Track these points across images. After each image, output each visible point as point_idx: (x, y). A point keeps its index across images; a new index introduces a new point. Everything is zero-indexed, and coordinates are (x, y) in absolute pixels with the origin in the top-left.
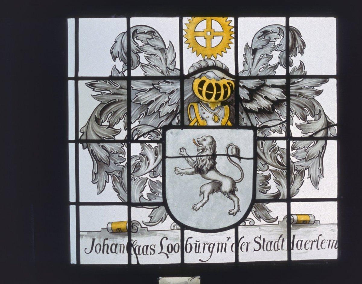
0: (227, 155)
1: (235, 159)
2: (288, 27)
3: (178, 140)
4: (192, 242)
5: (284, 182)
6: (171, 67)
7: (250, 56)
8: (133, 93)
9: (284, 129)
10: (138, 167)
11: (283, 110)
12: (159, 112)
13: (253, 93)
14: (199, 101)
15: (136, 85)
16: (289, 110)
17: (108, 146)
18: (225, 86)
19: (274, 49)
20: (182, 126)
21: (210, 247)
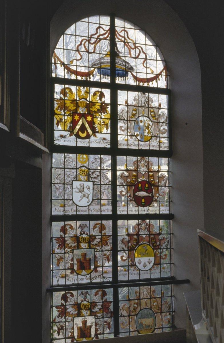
0: (87, 188)
1: (88, 189)
2: (101, 158)
3: (76, 184)
4: (79, 209)
5: (100, 195)
6: (74, 166)
7: (92, 164)
8: (65, 172)
9: (99, 182)
10: (66, 190)
11: (99, 178)
12: (71, 177)
13: (93, 173)
14: (80, 175)
15: (66, 170)
16: (101, 178)
17: (59, 185)
18: (86, 171)
19: (97, 163)
20: (76, 180)
21: (83, 211)
